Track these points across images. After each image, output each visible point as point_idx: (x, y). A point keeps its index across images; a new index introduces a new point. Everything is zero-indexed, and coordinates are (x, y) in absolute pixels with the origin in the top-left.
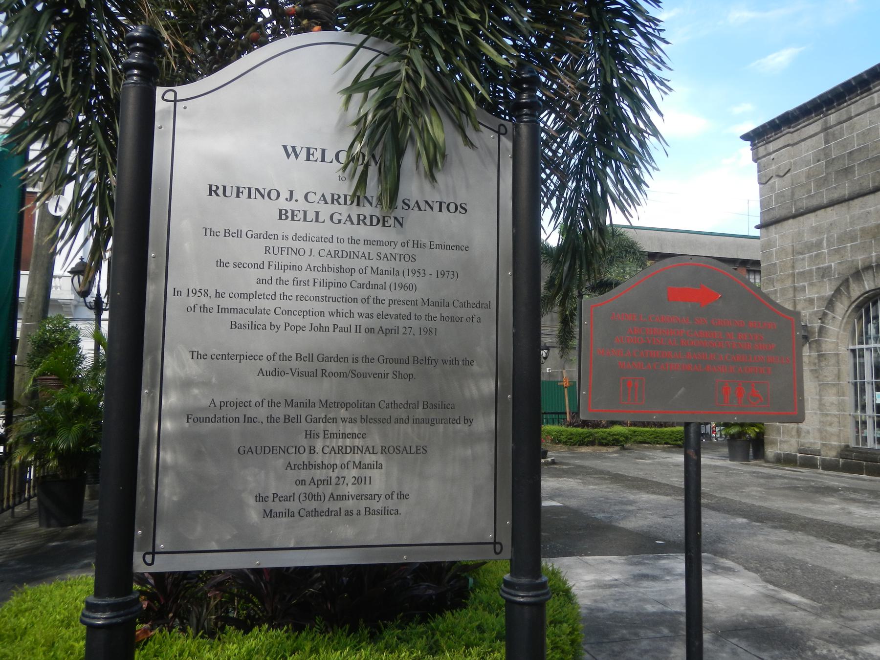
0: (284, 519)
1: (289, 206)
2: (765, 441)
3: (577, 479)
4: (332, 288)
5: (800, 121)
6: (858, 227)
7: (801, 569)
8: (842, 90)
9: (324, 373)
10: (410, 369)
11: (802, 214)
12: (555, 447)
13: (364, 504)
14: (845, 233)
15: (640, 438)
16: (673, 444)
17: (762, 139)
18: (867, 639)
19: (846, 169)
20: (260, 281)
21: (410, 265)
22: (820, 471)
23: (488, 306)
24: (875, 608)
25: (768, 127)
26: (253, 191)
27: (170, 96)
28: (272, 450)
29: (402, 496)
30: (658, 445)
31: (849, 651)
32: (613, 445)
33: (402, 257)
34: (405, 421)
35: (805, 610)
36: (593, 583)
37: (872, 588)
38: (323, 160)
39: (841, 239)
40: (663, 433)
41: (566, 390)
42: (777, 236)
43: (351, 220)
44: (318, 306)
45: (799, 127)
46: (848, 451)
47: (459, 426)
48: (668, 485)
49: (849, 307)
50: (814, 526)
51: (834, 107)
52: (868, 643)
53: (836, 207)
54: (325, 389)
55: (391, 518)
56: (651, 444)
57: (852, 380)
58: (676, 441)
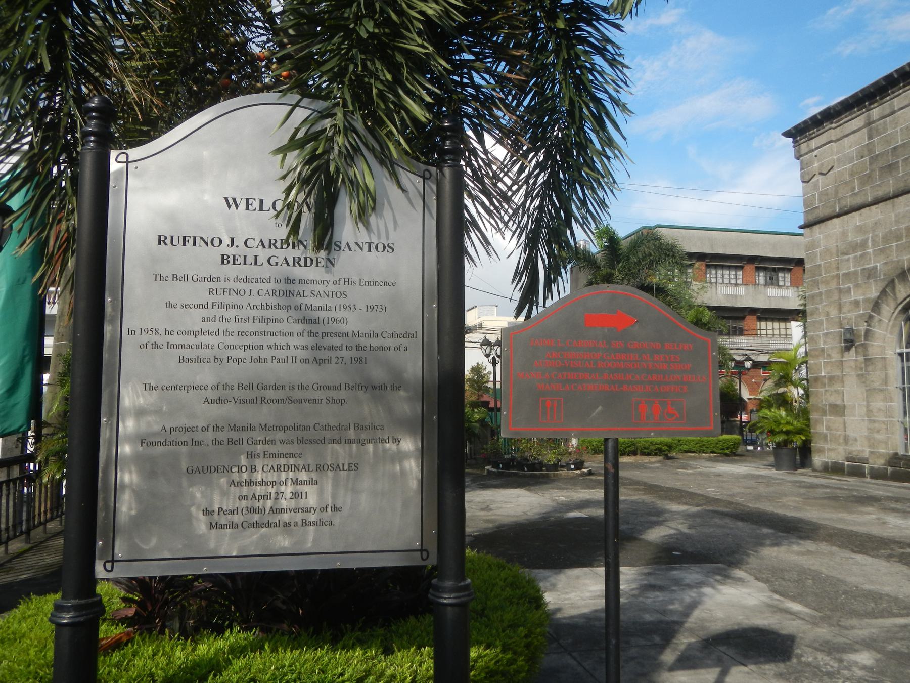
0: (228, 531)
1: (231, 251)
2: (812, 449)
4: (271, 324)
5: (843, 116)
6: (904, 226)
7: (813, 579)
8: (884, 83)
9: (263, 399)
10: (342, 394)
11: (846, 213)
13: (299, 517)
14: (891, 232)
15: (685, 447)
18: (857, 647)
19: (890, 165)
20: (205, 320)
21: (342, 301)
22: (868, 480)
23: (415, 336)
24: (876, 618)
26: (198, 240)
27: (123, 158)
28: (217, 470)
29: (335, 509)
31: (835, 658)
32: (656, 455)
33: (334, 294)
34: (338, 442)
35: (803, 619)
36: (598, 594)
37: (880, 598)
38: (261, 209)
39: (886, 239)
42: (821, 236)
43: (287, 262)
44: (256, 340)
45: (841, 122)
46: (896, 458)
47: (388, 445)
48: (702, 495)
49: (896, 308)
50: (842, 537)
51: (876, 101)
52: (856, 651)
53: (881, 204)
54: (265, 414)
55: (326, 529)
57: (900, 384)
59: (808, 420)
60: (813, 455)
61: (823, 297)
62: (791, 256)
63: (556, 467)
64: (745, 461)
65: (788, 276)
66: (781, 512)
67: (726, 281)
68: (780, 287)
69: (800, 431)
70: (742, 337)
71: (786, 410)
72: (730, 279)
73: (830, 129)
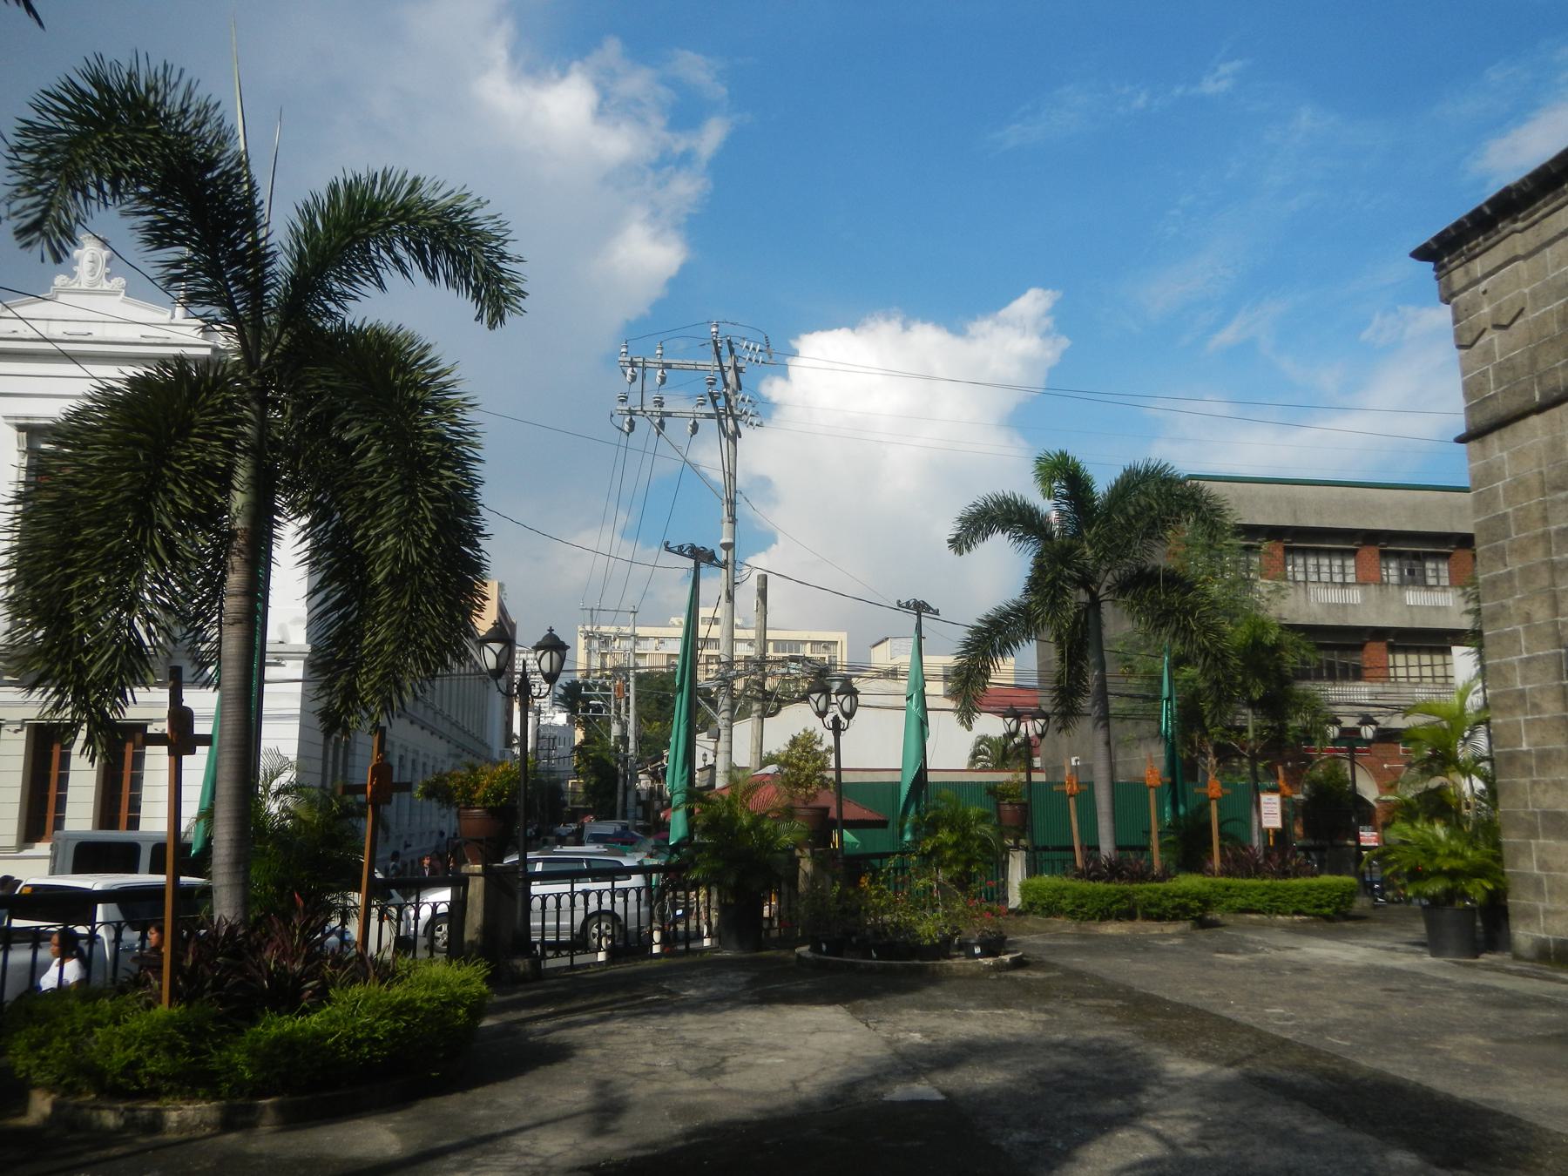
2: (1511, 911)
3: (1039, 1010)
5: (1539, 204)
12: (1049, 922)
16: (1313, 915)
17: (1458, 252)
25: (1469, 225)
30: (1279, 917)
32: (1175, 918)
40: (1288, 890)
41: (1072, 801)
42: (1505, 454)
45: (1537, 216)
48: (1250, 1029)
56: (1264, 913)
58: (1320, 906)
59: (1497, 845)
60: (1513, 923)
61: (1517, 583)
62: (1448, 530)
63: (943, 948)
64: (1366, 933)
65: (1444, 567)
66: (1440, 1083)
67: (1325, 577)
68: (1429, 588)
69: (1480, 872)
70: (1360, 683)
71: (1447, 824)
72: (1331, 573)
73: (1513, 232)
